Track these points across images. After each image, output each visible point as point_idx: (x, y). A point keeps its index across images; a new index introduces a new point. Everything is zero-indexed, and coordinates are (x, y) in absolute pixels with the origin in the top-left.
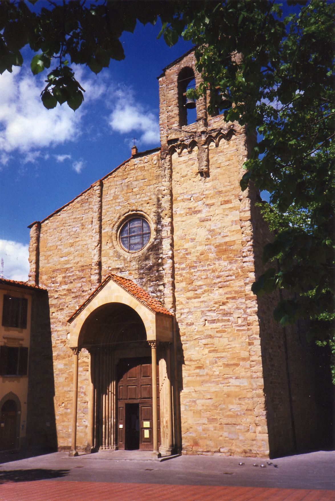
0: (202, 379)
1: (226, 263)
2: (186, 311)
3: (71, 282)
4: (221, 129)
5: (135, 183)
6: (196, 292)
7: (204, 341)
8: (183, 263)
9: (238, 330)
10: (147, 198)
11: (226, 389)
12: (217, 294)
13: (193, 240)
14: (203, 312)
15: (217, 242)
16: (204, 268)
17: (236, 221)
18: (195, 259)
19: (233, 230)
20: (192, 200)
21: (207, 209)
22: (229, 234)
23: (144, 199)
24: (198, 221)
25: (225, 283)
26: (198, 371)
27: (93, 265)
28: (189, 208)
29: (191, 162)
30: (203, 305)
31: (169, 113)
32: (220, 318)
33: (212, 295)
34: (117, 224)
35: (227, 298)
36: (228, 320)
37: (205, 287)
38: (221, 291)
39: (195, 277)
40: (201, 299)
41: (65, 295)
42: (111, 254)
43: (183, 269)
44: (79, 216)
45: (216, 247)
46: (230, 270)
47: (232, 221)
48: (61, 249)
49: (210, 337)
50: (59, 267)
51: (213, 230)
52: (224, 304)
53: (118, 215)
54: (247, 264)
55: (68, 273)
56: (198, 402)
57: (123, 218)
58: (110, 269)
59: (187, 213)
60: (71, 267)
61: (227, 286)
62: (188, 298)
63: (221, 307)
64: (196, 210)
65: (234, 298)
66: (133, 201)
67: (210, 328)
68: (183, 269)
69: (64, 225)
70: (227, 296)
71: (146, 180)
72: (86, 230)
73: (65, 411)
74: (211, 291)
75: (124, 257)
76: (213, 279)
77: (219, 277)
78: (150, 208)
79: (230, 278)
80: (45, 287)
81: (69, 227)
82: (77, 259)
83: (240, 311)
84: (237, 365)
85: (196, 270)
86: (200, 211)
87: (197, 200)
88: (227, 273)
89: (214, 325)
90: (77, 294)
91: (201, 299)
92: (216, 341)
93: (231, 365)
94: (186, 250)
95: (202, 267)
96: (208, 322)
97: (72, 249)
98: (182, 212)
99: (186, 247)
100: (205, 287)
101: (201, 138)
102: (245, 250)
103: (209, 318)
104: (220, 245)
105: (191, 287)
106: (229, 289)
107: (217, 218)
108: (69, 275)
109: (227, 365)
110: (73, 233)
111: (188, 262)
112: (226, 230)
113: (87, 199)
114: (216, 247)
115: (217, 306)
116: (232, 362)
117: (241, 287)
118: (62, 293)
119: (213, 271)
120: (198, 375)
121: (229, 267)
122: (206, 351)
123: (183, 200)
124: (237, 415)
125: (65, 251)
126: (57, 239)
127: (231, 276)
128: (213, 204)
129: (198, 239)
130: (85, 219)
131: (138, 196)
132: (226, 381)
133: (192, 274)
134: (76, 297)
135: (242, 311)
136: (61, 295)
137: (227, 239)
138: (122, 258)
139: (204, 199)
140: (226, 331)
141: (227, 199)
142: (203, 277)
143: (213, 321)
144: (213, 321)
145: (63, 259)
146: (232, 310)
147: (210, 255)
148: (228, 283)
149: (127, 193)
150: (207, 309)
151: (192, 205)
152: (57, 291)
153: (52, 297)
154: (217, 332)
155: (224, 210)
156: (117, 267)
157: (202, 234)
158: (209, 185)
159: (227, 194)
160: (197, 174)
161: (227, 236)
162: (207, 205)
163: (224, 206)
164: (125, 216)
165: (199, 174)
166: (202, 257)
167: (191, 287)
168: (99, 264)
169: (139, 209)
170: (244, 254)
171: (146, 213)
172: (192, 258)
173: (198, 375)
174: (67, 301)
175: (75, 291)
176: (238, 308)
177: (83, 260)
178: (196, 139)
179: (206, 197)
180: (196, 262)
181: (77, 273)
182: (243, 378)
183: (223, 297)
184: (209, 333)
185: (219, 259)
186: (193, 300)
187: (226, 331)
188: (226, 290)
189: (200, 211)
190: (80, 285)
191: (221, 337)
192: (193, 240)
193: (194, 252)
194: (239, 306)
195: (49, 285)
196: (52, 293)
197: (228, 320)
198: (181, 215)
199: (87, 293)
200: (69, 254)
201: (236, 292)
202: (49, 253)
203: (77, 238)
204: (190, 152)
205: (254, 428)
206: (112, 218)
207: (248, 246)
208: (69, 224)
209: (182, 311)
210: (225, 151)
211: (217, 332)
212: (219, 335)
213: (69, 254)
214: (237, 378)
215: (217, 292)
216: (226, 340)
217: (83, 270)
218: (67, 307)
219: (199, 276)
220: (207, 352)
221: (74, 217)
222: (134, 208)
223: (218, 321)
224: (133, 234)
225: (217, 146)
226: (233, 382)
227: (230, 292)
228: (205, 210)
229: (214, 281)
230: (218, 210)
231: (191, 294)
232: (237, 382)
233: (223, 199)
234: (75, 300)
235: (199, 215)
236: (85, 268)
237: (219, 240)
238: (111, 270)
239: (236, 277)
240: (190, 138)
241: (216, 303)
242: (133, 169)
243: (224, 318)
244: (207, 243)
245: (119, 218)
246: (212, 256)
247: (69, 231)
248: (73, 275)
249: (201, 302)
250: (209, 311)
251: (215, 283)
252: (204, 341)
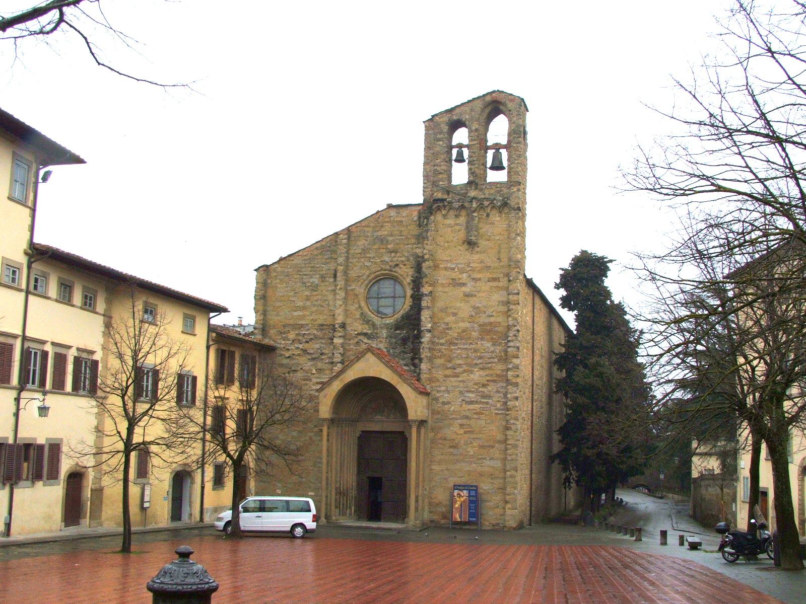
0: (455, 457)
1: (489, 345)
2: (443, 388)
3: (307, 342)
4: (495, 199)
5: (391, 238)
6: (455, 371)
7: (459, 421)
8: (443, 338)
9: (496, 414)
10: (403, 259)
11: (479, 469)
12: (477, 375)
13: (455, 314)
14: (461, 392)
15: (481, 321)
16: (465, 347)
17: (502, 302)
18: (455, 335)
19: (499, 310)
20: (456, 270)
21: (472, 283)
22: (494, 314)
23: (400, 259)
24: (462, 295)
25: (487, 365)
26: (451, 450)
27: (337, 326)
28: (453, 279)
29: (457, 228)
30: (461, 384)
31: (436, 167)
32: (479, 400)
33: (472, 376)
34: (366, 282)
35: (488, 381)
36: (487, 403)
37: (465, 367)
38: (481, 372)
39: (455, 355)
40: (460, 379)
41: (299, 355)
42: (358, 316)
43: (442, 344)
44: (318, 266)
45: (480, 326)
46: (492, 352)
47: (499, 302)
48: (294, 301)
49: (467, 417)
50: (291, 322)
51: (478, 308)
52: (484, 386)
53: (368, 272)
54: (512, 349)
55: (302, 331)
56: (450, 479)
57: (373, 276)
58: (356, 333)
59: (450, 284)
60: (307, 324)
61: (489, 368)
62: (446, 376)
63: (481, 389)
64: (460, 281)
65: (494, 381)
66: (387, 259)
67: (466, 409)
68: (442, 344)
69: (300, 273)
70: (488, 378)
71: (403, 237)
72: (327, 283)
73: (300, 479)
74: (471, 372)
75: (373, 322)
76: (474, 359)
77: (480, 358)
78: (406, 270)
79: (492, 360)
80: (273, 342)
81: (305, 277)
82: (314, 317)
83: (499, 395)
84: (492, 447)
85: (456, 347)
86: (464, 284)
87: (462, 271)
89: (471, 407)
90: (314, 356)
91: (460, 379)
92: (473, 422)
93: (486, 446)
94: (447, 324)
95: (464, 344)
96: (466, 403)
97: (308, 303)
98: (444, 282)
99: (446, 320)
100: (465, 367)
101: (472, 205)
102: (511, 335)
104: (484, 325)
105: (450, 365)
106: (491, 372)
108: (303, 332)
109: (482, 447)
110: (309, 284)
111: (449, 337)
112: (492, 310)
113: (329, 247)
114: (480, 326)
115: (476, 387)
116: (486, 444)
117: (503, 371)
118: (296, 353)
119: (475, 351)
120: (452, 454)
121: (492, 349)
122: (462, 431)
123: (446, 269)
124: (489, 492)
125: (300, 304)
126: (289, 288)
127: (494, 358)
128: (480, 279)
129: (461, 315)
130: (326, 270)
131: (393, 254)
132: (480, 461)
133: (451, 350)
134: (313, 359)
135: (502, 395)
136: (293, 354)
137: (492, 320)
138: (370, 323)
139: (470, 272)
140: (483, 414)
141: (495, 276)
142: (464, 356)
143: (471, 402)
144: (471, 402)
145: (296, 314)
146: (492, 394)
147: (473, 333)
148: (490, 365)
149: (379, 248)
150: (466, 389)
151: (454, 275)
152: (288, 349)
153: (281, 355)
154: (474, 413)
155: (491, 287)
156: (365, 331)
157: (465, 309)
158: (476, 257)
159: (495, 271)
160: (463, 243)
161: (492, 316)
162: (474, 279)
163: (491, 284)
164: (375, 274)
165: (466, 243)
166: (464, 335)
167: (450, 365)
168: (343, 326)
169: (394, 270)
170: (510, 339)
171: (401, 275)
172: (453, 334)
173: (452, 454)
174: (301, 362)
175: (312, 352)
176: (498, 392)
177: (322, 318)
178: (466, 204)
179: (473, 270)
180: (456, 339)
181: (315, 332)
182: (497, 459)
183: (483, 379)
184: (468, 414)
185: (482, 339)
186: (452, 379)
187: (483, 414)
188: (488, 372)
189: (464, 284)
190: (317, 346)
191: (478, 419)
192: (455, 314)
193: (455, 328)
194: (499, 389)
195: (279, 341)
196: (283, 351)
197: (487, 403)
198: (443, 285)
199: (326, 357)
200: (304, 308)
201: (497, 375)
202: (278, 304)
203: (315, 291)
204: (457, 216)
205: (503, 505)
206: (360, 275)
207: (515, 331)
208: (305, 273)
209: (438, 389)
210: (496, 223)
211: (474, 413)
212: (475, 416)
213: (304, 308)
214: (491, 459)
215: (477, 373)
216: (483, 422)
217: (321, 330)
218: (301, 369)
219: (458, 354)
220: (462, 433)
221: (312, 265)
222: (388, 267)
223: (477, 402)
224: (383, 296)
225: (488, 215)
226: (487, 462)
227: (491, 375)
228: (471, 284)
229: (475, 361)
230: (485, 287)
231: (448, 372)
232: (492, 463)
233: (490, 276)
234: (311, 363)
235: (463, 289)
236: (325, 327)
237: (483, 319)
238: (357, 334)
239: (498, 360)
240: (459, 202)
241: (476, 384)
242: (388, 222)
243: (482, 400)
244: (470, 320)
245: (368, 276)
246: (475, 334)
247: (304, 280)
248: (309, 334)
249: (459, 381)
250: (468, 391)
251: (476, 364)
252: (459, 421)
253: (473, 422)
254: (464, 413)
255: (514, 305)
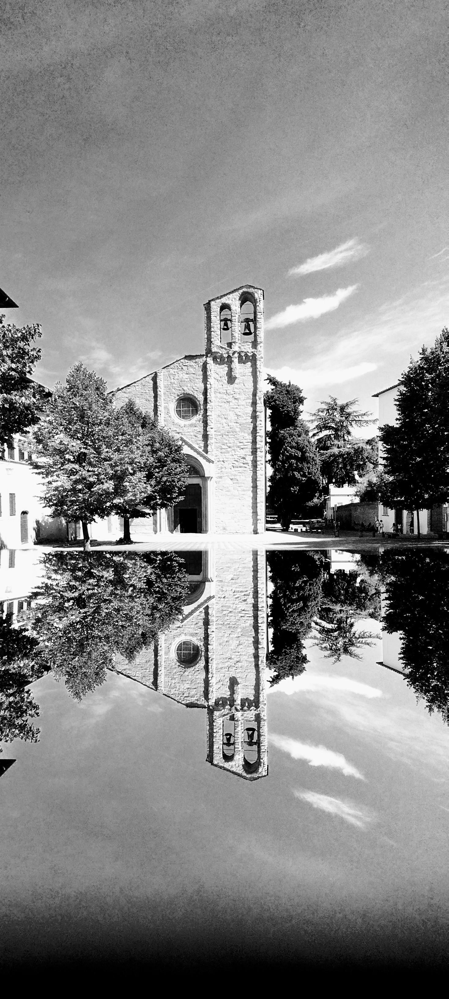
5: (188, 375)
26: (227, 493)
30: (231, 457)
43: (220, 435)
49: (235, 475)
68: (220, 435)
70: (246, 453)
88: (246, 441)
89: (237, 469)
103: (234, 465)
104: (243, 424)
107: (242, 407)
156: (175, 429)
186: (225, 454)
223: (240, 467)
253: (238, 477)
254: (232, 473)
255: (260, 412)
